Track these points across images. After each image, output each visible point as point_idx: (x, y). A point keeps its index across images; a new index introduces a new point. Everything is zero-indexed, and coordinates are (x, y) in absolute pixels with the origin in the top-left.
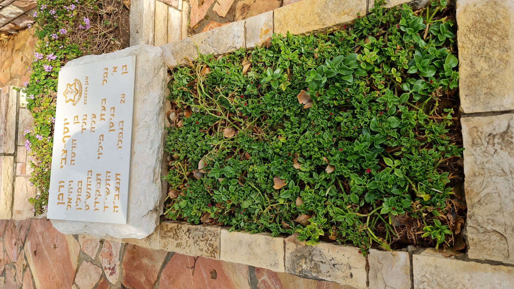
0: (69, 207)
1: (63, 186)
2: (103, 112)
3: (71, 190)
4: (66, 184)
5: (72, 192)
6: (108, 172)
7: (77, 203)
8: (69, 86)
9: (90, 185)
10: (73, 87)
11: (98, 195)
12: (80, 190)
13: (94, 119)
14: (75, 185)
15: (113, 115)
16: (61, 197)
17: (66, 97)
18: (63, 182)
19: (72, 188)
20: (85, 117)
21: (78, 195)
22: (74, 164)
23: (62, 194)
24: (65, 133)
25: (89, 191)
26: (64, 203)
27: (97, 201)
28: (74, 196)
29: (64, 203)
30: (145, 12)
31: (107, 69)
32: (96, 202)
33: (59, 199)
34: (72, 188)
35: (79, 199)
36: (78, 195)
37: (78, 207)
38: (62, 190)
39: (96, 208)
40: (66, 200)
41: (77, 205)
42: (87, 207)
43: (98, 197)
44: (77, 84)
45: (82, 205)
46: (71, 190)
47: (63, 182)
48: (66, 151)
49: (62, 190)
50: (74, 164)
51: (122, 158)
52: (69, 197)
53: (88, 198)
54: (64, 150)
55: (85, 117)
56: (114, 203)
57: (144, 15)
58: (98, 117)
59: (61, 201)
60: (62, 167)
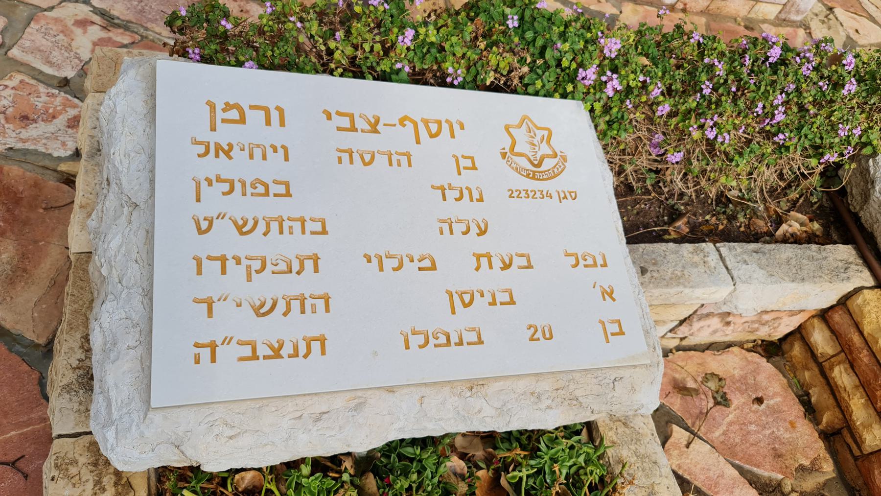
0: (201, 149)
1: (268, 123)
2: (497, 263)
3: (258, 153)
4: (274, 135)
5: (251, 157)
6: (327, 299)
7: (219, 179)
8: (546, 133)
9: (303, 312)
10: (545, 149)
11: (249, 267)
12: (261, 189)
13: (474, 230)
14: (271, 169)
15: (493, 303)
16: (234, 114)
17: (520, 126)
18: (282, 123)
19: (264, 158)
20: (476, 196)
21: (244, 184)
22: (340, 160)
23: (242, 120)
24: (426, 122)
25: (281, 306)
26: (213, 129)
27: (231, 264)
28: (238, 167)
29: (213, 129)
30: (687, 291)
31: (605, 265)
32: (223, 260)
33: (228, 107)
34: (264, 158)
35: (232, 190)
36: (244, 184)
37: (204, 184)
38: (255, 118)
39: (205, 262)
40: (225, 135)
41: (210, 183)
42: (204, 225)
43: (242, 268)
44: (555, 161)
45: (214, 201)
46: (258, 153)
47: (282, 123)
48: (376, 131)
49: (255, 118)
50: (340, 160)
51: (375, 353)
52: (236, 149)
53: (235, 223)
54: (377, 121)
55: (476, 196)
56: (227, 341)
57: (680, 288)
58: (482, 245)
59: (220, 115)
60: (329, 117)
